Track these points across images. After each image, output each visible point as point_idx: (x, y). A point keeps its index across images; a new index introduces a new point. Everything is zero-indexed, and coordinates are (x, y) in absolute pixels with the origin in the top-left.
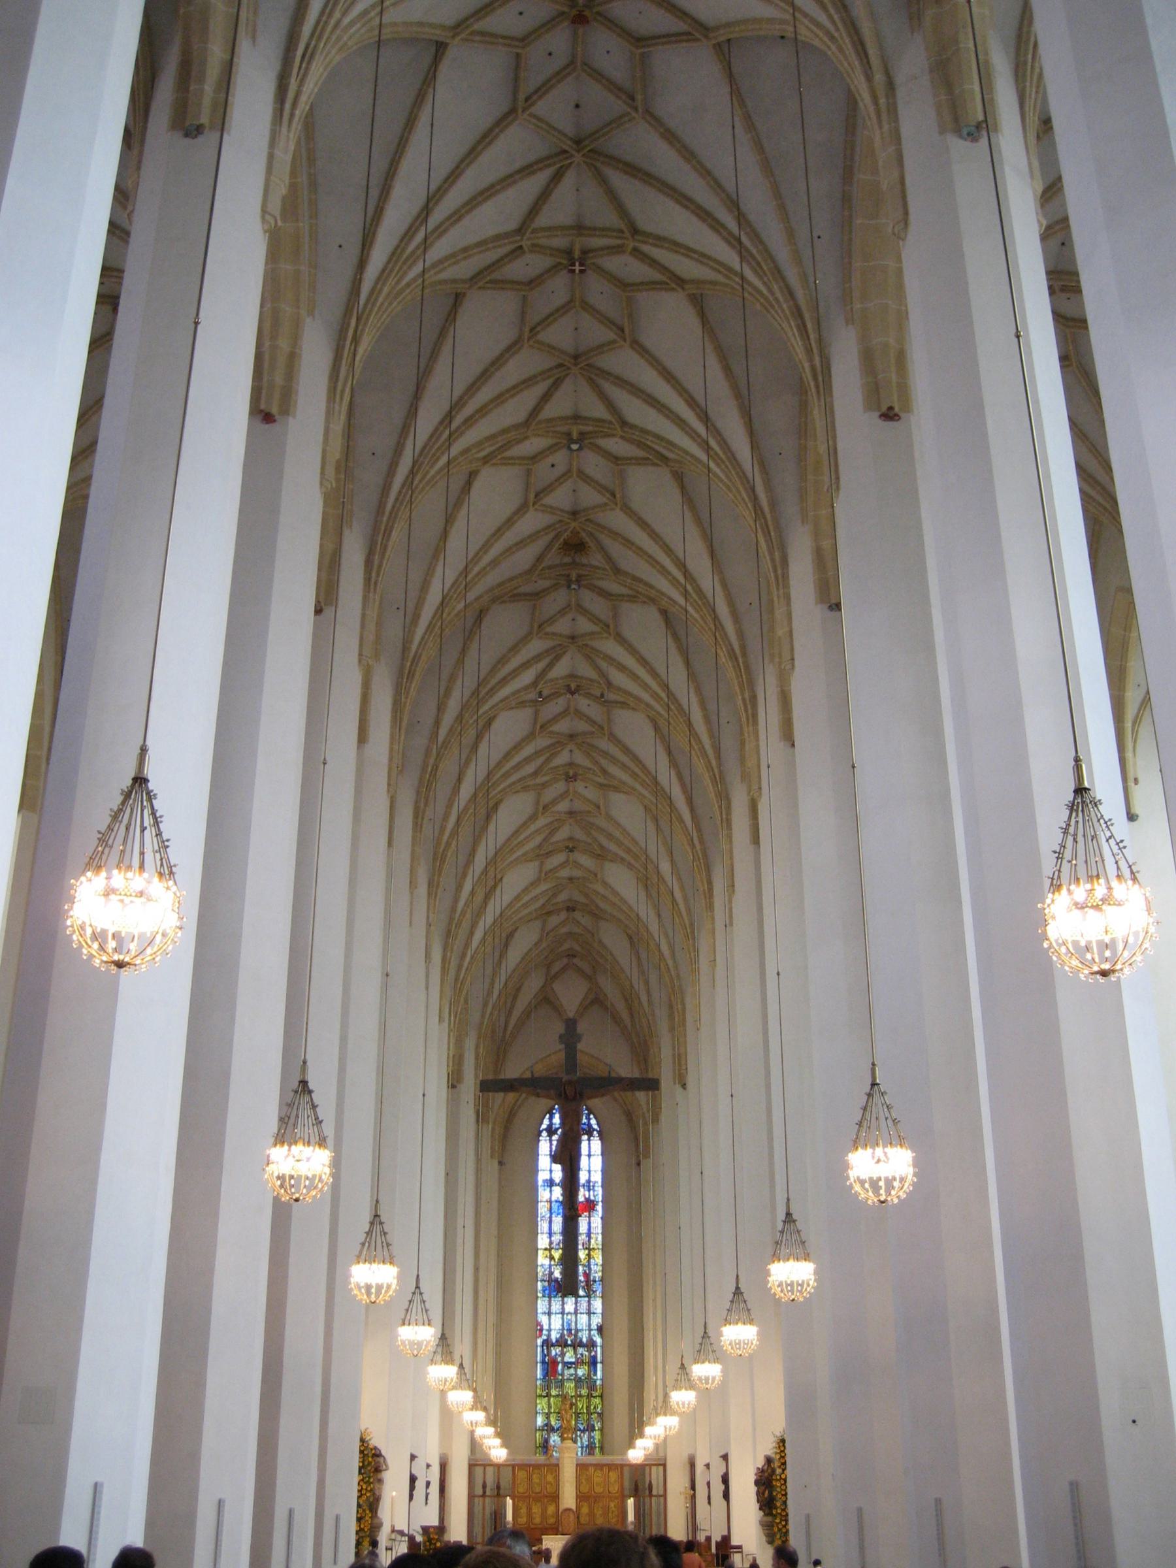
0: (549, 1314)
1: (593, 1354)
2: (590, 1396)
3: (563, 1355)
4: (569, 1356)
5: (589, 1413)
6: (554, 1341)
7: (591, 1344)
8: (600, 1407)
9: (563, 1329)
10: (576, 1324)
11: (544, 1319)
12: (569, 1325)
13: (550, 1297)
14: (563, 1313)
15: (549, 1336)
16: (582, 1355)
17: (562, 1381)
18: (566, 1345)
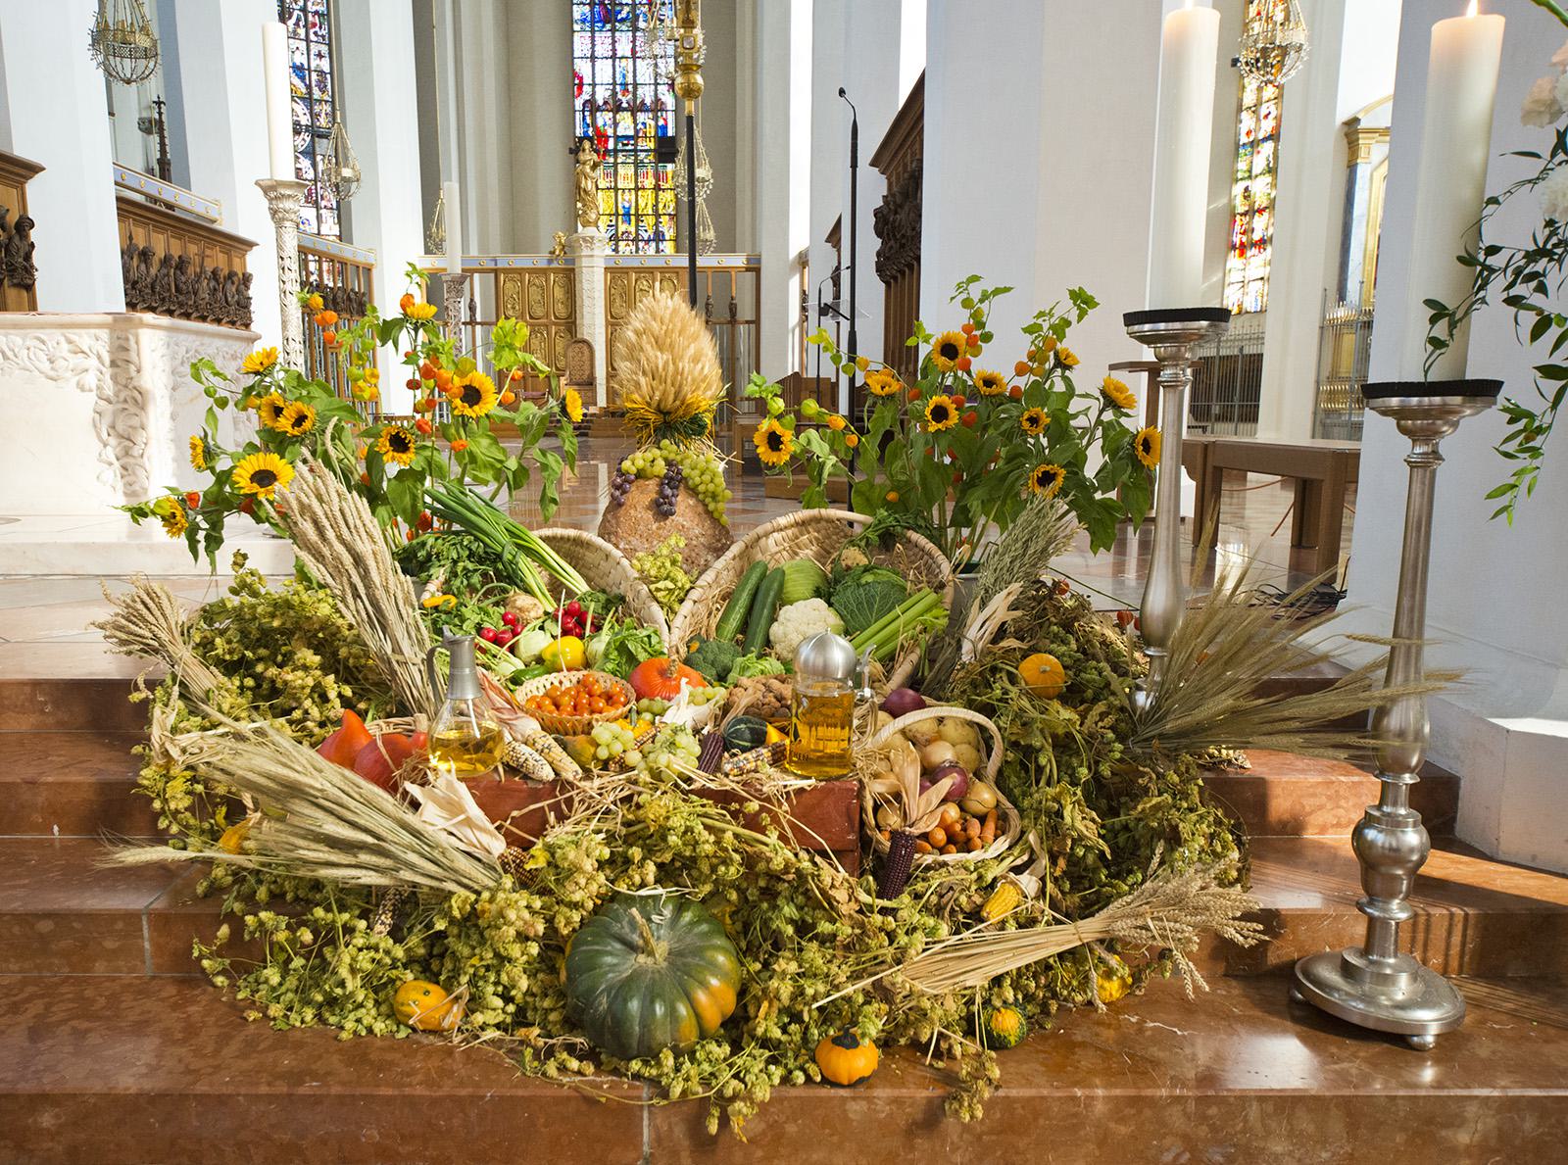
0: (593, 58)
1: (661, 122)
2: (657, 188)
3: (616, 124)
4: (626, 125)
5: (657, 215)
6: (600, 102)
7: (658, 107)
8: (672, 205)
9: (614, 84)
10: (635, 76)
11: (583, 67)
12: (624, 76)
13: (593, 32)
14: (614, 57)
15: (593, 94)
16: (644, 124)
17: (615, 164)
18: (617, 108)
